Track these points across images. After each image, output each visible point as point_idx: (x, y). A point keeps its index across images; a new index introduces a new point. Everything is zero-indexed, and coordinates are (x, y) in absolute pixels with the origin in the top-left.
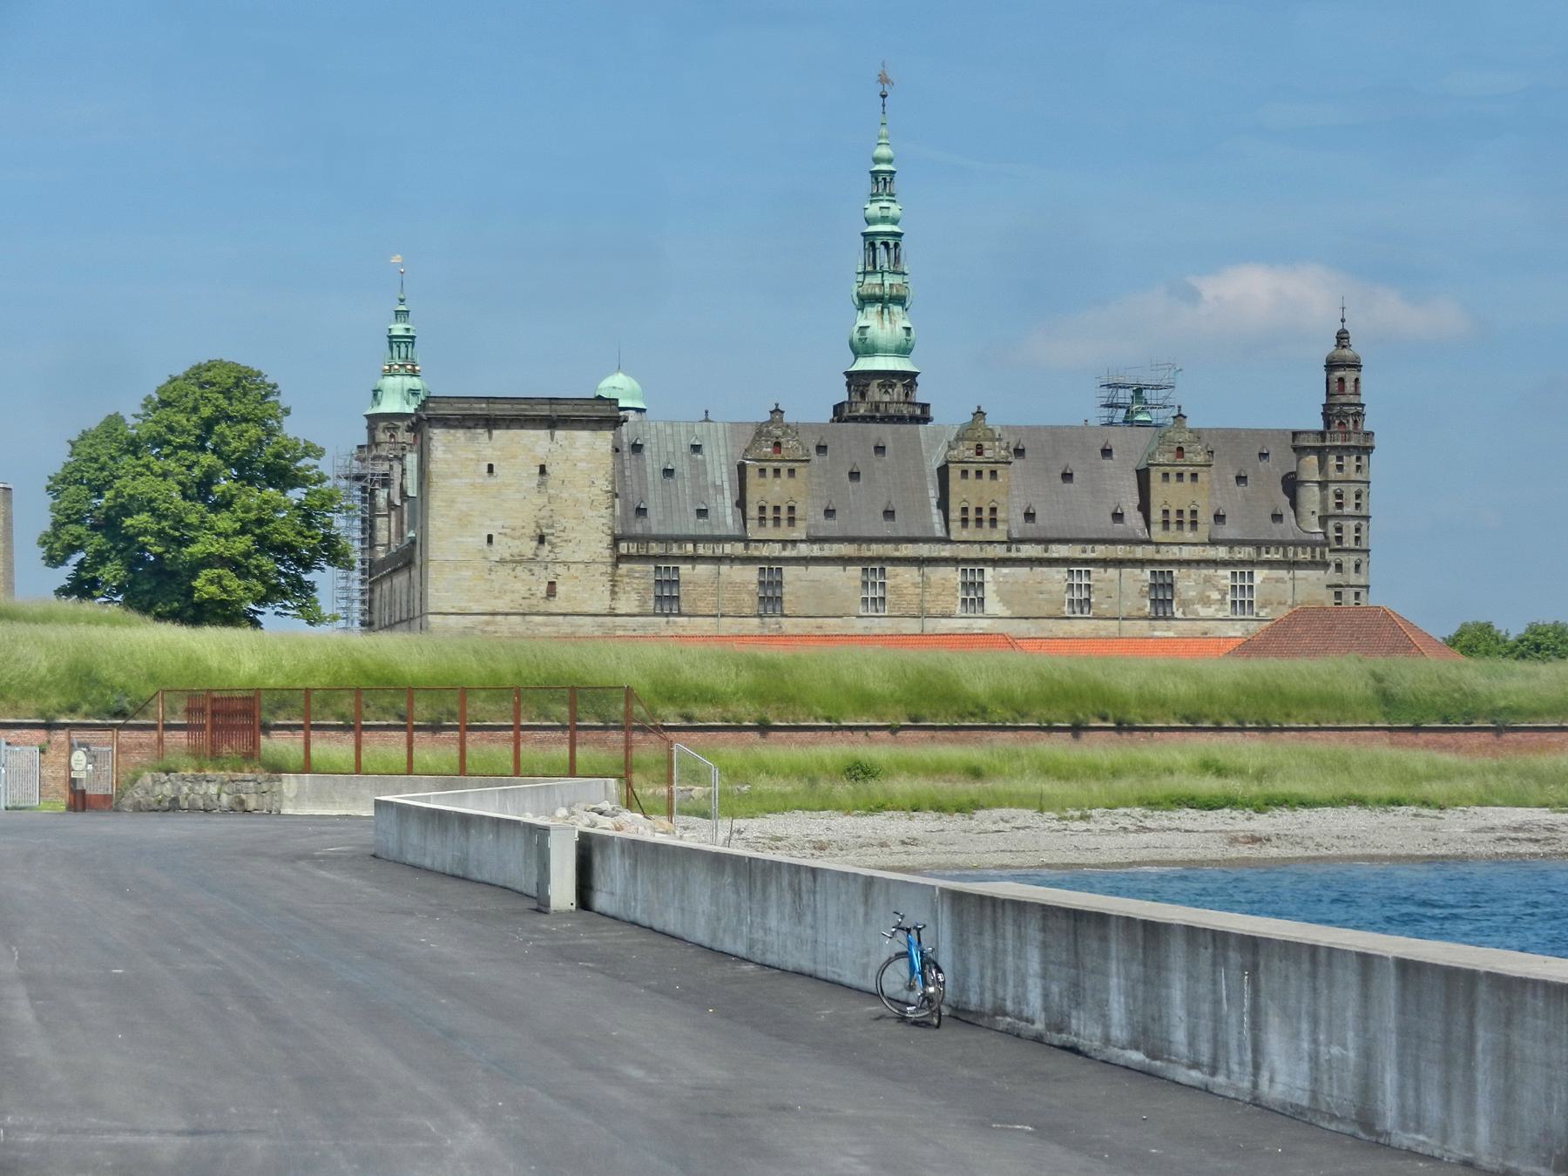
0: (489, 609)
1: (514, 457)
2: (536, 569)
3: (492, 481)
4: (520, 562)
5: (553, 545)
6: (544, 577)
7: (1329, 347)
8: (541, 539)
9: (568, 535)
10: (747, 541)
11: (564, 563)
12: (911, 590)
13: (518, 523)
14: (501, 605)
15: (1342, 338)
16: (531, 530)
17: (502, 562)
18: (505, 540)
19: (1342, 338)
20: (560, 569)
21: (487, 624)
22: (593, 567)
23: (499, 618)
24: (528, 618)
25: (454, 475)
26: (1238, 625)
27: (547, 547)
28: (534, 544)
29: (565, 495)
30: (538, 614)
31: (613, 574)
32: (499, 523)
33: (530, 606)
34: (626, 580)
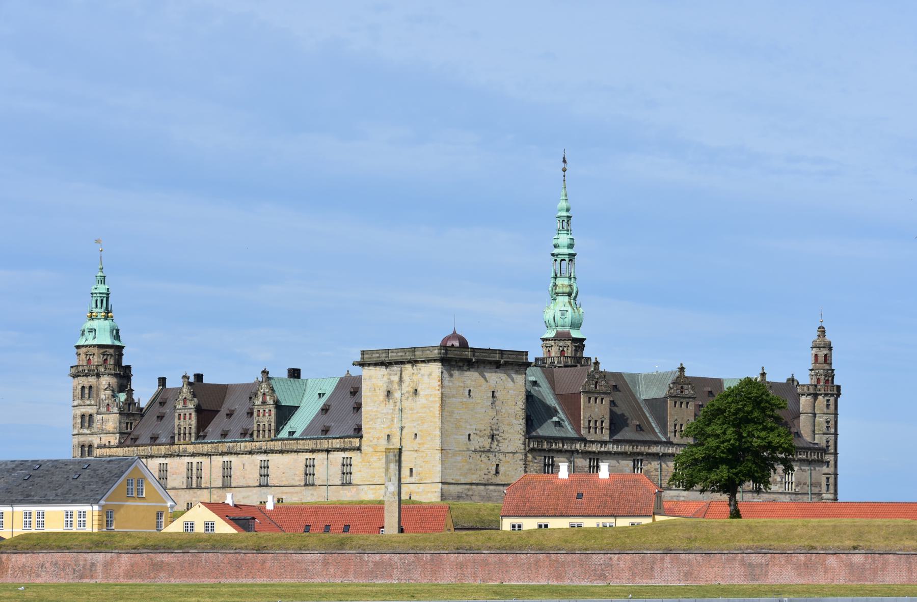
0: (469, 481)
1: (480, 386)
2: (491, 456)
3: (471, 400)
4: (483, 452)
5: (498, 441)
6: (494, 461)
7: (814, 335)
8: (492, 437)
9: (506, 435)
10: (584, 440)
11: (504, 453)
12: (654, 473)
13: (482, 427)
14: (474, 478)
15: (822, 331)
16: (488, 432)
17: (475, 451)
18: (477, 437)
19: (822, 331)
20: (501, 456)
21: (469, 490)
22: (516, 455)
23: (474, 487)
24: (487, 487)
25: (453, 396)
26: (788, 496)
27: (496, 443)
28: (490, 440)
29: (504, 411)
30: (492, 484)
31: (525, 460)
32: (474, 427)
33: (488, 479)
34: (531, 464)
